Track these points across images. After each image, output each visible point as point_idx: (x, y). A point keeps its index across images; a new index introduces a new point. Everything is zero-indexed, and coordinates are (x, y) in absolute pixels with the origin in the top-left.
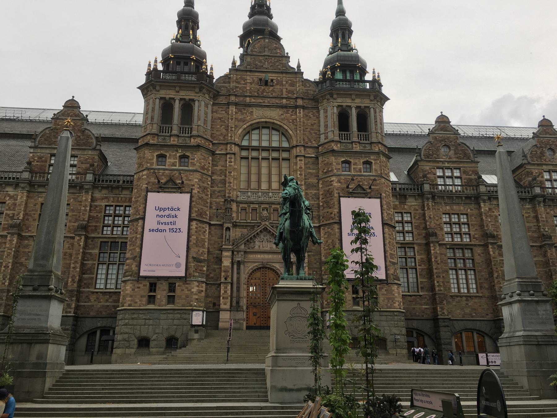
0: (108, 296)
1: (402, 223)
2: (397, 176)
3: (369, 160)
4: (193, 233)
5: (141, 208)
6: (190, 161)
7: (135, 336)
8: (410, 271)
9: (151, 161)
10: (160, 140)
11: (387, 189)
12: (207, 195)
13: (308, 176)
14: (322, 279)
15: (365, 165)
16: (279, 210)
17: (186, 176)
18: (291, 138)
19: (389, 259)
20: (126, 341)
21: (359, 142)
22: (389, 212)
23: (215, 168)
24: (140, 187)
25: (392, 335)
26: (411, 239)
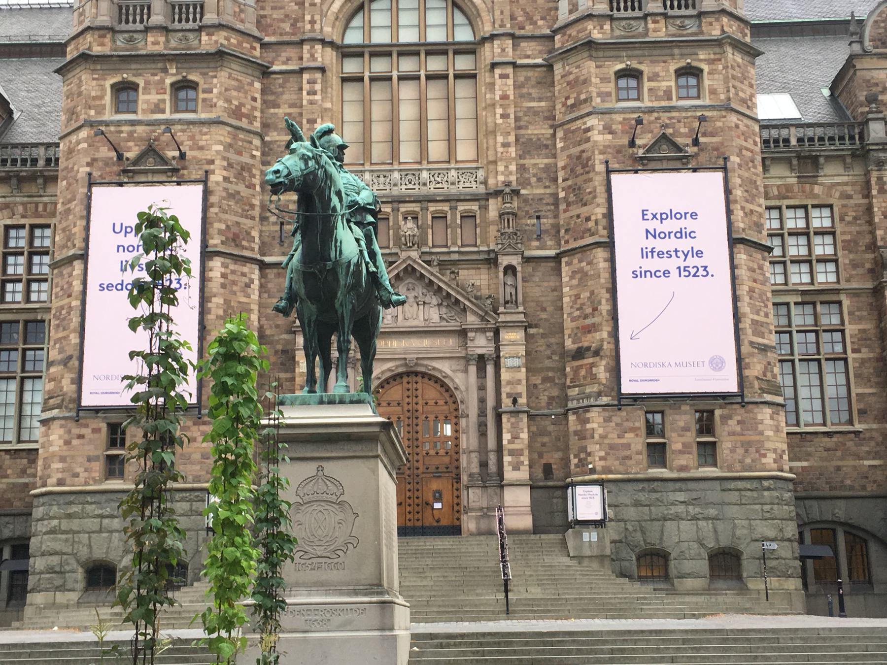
0: (25, 461)
1: (807, 234)
2: (800, 101)
3: (694, 64)
4: (214, 290)
5: (78, 230)
6: (202, 96)
7: (78, 561)
8: (827, 367)
9: (98, 102)
10: (119, 43)
11: (744, 144)
12: (251, 186)
13: (526, 118)
14: (566, 398)
15: (682, 81)
16: (449, 218)
17: (192, 138)
18: (479, 15)
19: (749, 336)
20: (55, 572)
21: (665, 16)
22: (751, 207)
23: (272, 111)
24: (73, 174)
25: (757, 540)
26: (832, 278)
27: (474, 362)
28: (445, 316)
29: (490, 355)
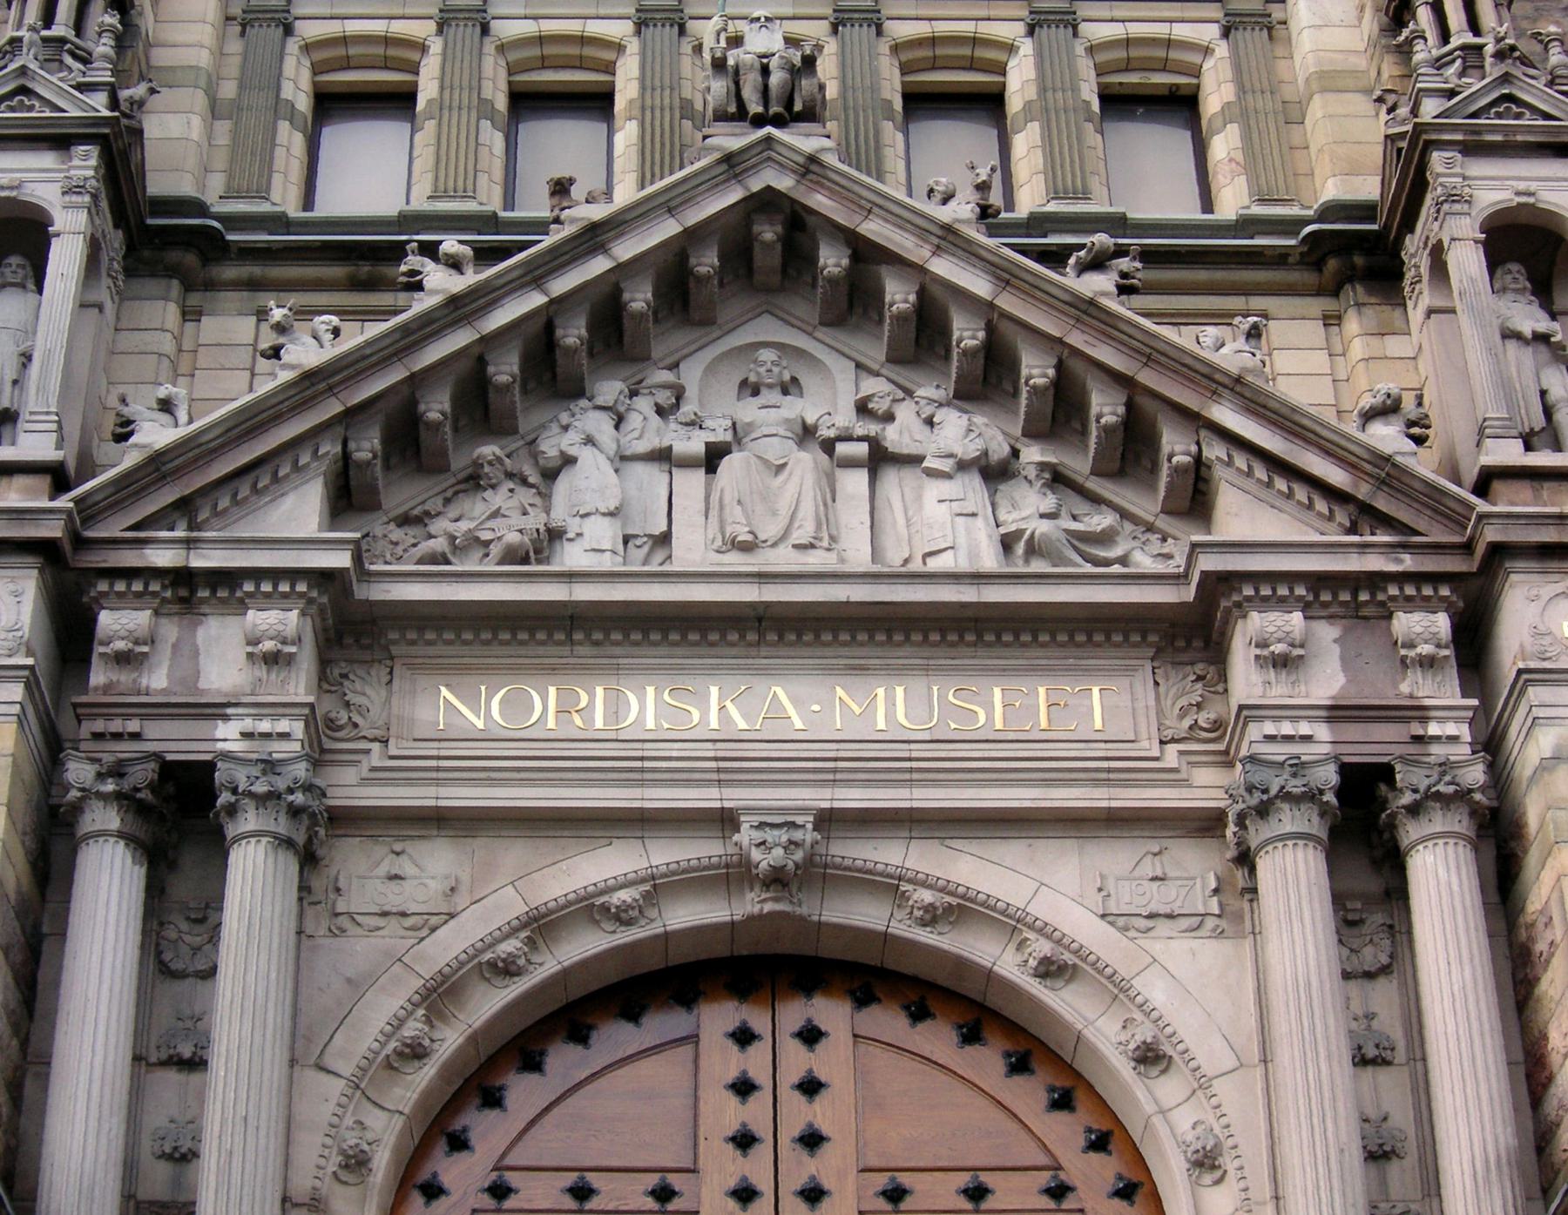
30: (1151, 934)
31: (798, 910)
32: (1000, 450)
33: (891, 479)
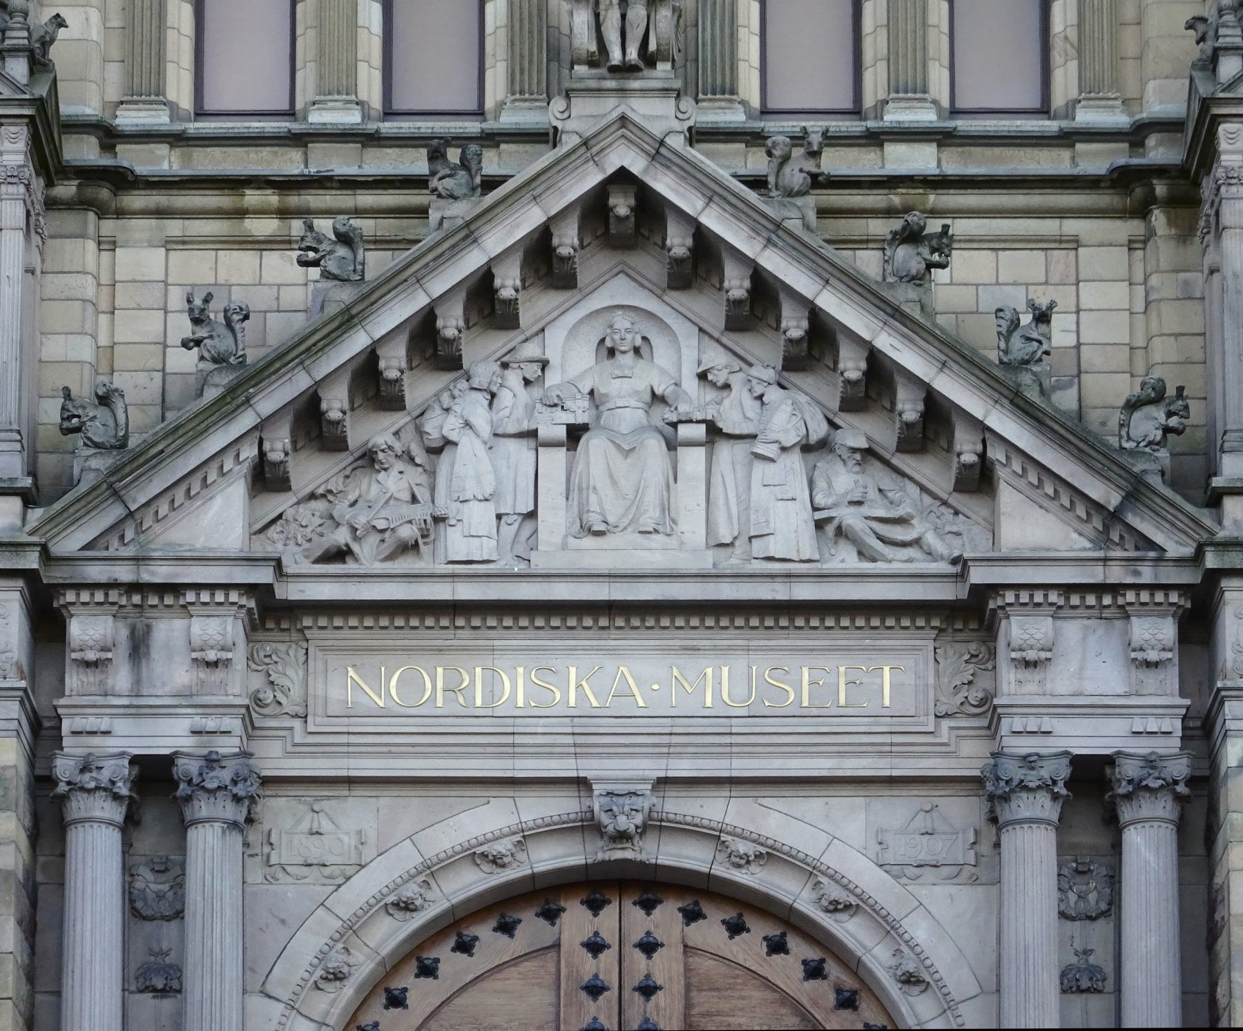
27: (1044, 807)
28: (851, 518)
29: (1150, 762)
30: (920, 881)
31: (639, 857)
32: (819, 429)
33: (725, 451)
